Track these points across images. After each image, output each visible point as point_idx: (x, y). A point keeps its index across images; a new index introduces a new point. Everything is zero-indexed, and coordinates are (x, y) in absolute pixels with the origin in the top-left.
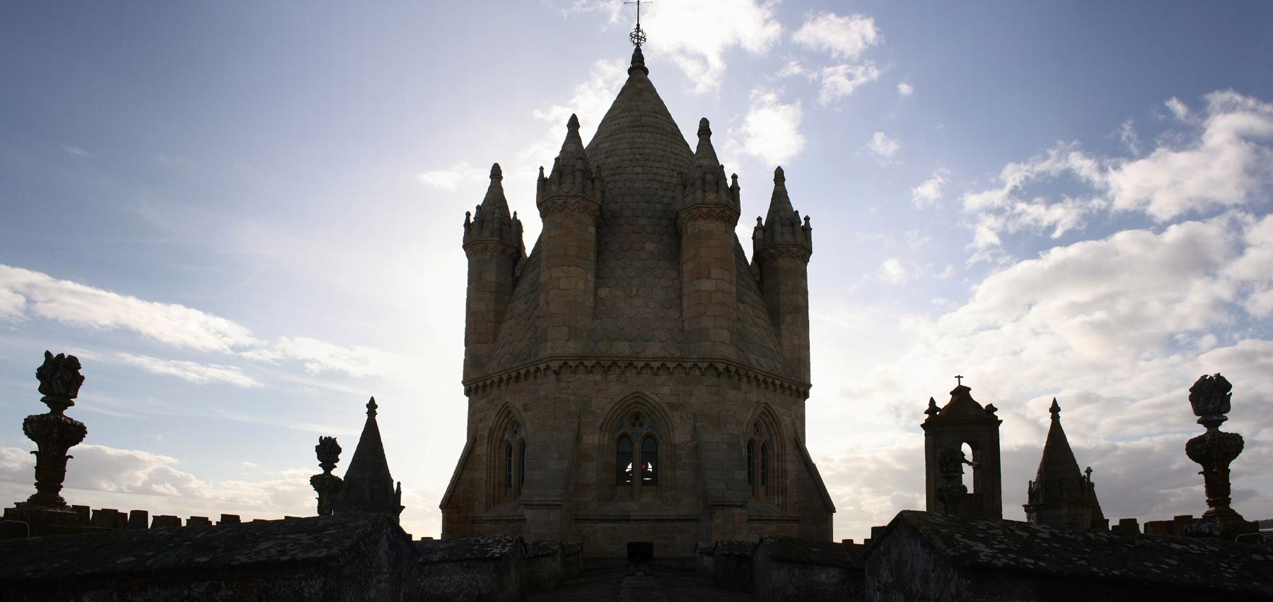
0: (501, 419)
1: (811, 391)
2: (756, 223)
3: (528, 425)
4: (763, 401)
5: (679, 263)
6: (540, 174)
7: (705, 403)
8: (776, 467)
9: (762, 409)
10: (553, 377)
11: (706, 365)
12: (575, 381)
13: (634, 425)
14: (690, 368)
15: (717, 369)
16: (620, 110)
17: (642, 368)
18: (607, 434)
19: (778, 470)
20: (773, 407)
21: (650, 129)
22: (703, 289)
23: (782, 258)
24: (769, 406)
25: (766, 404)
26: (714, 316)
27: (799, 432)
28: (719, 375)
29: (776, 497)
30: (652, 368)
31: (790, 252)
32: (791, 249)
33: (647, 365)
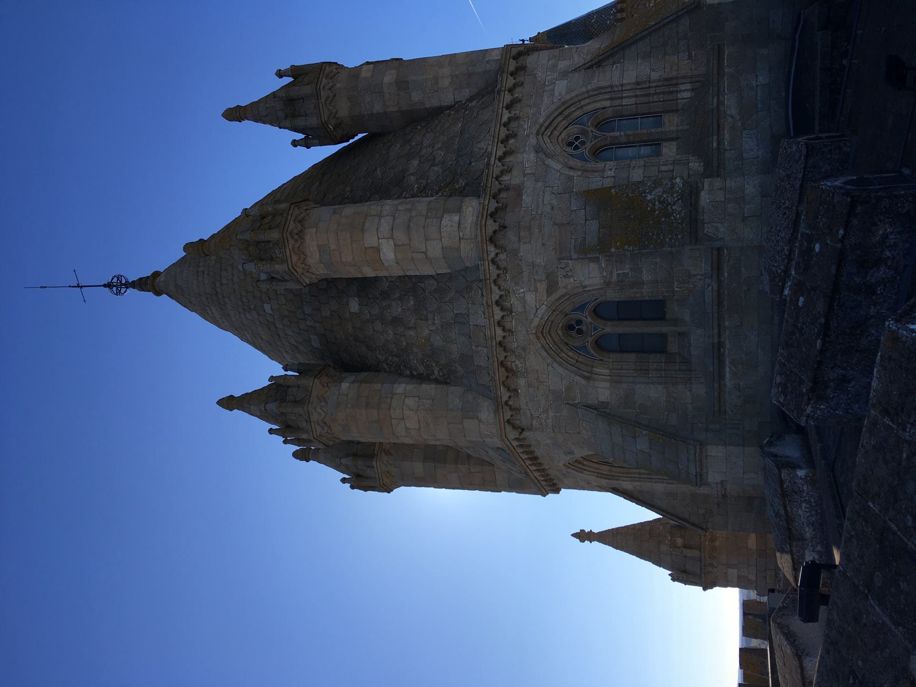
0: (586, 468)
4: (533, 141)
7: (543, 244)
8: (631, 101)
9: (546, 139)
10: (526, 434)
11: (491, 248)
12: (529, 409)
13: (580, 332)
15: (495, 232)
19: (636, 96)
20: (541, 120)
21: (218, 284)
23: (336, 112)
24: (541, 126)
25: (537, 134)
26: (426, 240)
28: (503, 227)
29: (679, 96)
30: (503, 317)
31: (329, 101)
32: (323, 101)
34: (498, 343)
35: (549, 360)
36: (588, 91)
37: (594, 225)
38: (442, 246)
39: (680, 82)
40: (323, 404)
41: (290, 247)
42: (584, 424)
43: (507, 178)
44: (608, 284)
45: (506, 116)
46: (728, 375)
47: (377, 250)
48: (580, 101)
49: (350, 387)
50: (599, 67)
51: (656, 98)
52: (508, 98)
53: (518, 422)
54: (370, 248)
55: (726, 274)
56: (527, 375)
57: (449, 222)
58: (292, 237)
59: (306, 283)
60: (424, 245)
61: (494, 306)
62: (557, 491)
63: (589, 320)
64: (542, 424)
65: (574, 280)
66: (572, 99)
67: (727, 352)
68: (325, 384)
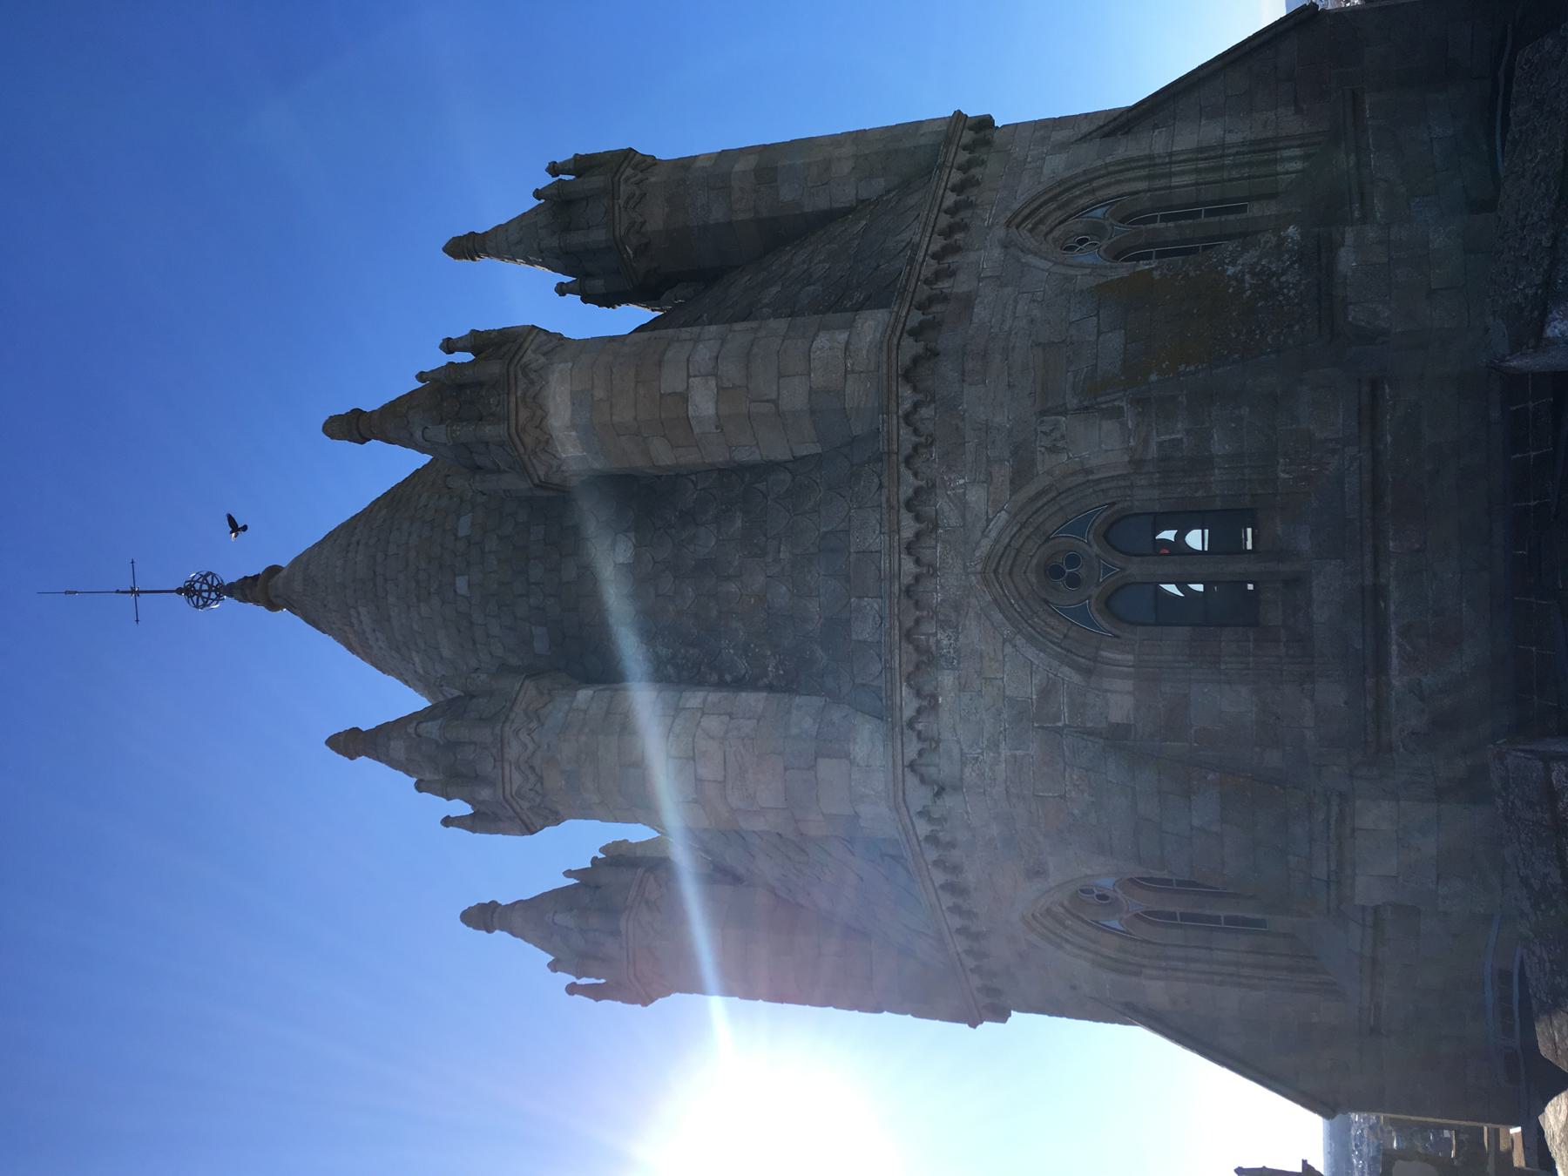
1: (972, 111)
2: (574, 300)
3: (1089, 872)
4: (1000, 232)
5: (659, 477)
6: (459, 826)
9: (1025, 233)
10: (949, 801)
11: (906, 392)
14: (916, 432)
15: (916, 360)
16: (346, 628)
17: (918, 562)
18: (1104, 654)
20: (1016, 206)
22: (712, 411)
23: (644, 223)
24: (1016, 214)
25: (1008, 224)
26: (780, 376)
27: (1085, 128)
28: (932, 354)
29: (1279, 169)
31: (632, 203)
32: (621, 202)
33: (910, 548)
34: (903, 588)
35: (1007, 631)
36: (1107, 166)
37: (1115, 340)
38: (810, 387)
39: (1281, 145)
40: (534, 725)
41: (519, 394)
42: (1075, 777)
43: (946, 285)
44: (1137, 464)
45: (951, 199)
46: (1395, 661)
47: (684, 398)
48: (1090, 181)
49: (592, 698)
50: (1127, 133)
51: (1235, 174)
52: (956, 177)
53: (933, 770)
54: (669, 394)
55: (1389, 439)
56: (959, 663)
57: (828, 343)
58: (525, 375)
59: (539, 477)
60: (775, 388)
61: (903, 511)
62: (1001, 1015)
63: (1096, 549)
64: (983, 775)
65: (1069, 458)
66: (1076, 176)
67: (1392, 609)
68: (546, 692)
